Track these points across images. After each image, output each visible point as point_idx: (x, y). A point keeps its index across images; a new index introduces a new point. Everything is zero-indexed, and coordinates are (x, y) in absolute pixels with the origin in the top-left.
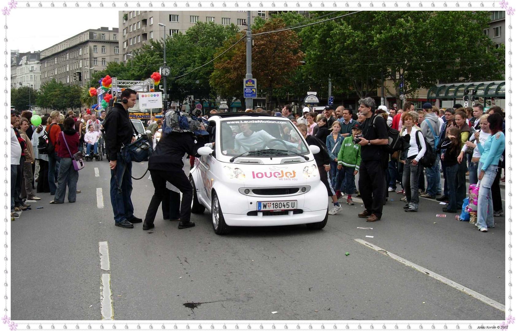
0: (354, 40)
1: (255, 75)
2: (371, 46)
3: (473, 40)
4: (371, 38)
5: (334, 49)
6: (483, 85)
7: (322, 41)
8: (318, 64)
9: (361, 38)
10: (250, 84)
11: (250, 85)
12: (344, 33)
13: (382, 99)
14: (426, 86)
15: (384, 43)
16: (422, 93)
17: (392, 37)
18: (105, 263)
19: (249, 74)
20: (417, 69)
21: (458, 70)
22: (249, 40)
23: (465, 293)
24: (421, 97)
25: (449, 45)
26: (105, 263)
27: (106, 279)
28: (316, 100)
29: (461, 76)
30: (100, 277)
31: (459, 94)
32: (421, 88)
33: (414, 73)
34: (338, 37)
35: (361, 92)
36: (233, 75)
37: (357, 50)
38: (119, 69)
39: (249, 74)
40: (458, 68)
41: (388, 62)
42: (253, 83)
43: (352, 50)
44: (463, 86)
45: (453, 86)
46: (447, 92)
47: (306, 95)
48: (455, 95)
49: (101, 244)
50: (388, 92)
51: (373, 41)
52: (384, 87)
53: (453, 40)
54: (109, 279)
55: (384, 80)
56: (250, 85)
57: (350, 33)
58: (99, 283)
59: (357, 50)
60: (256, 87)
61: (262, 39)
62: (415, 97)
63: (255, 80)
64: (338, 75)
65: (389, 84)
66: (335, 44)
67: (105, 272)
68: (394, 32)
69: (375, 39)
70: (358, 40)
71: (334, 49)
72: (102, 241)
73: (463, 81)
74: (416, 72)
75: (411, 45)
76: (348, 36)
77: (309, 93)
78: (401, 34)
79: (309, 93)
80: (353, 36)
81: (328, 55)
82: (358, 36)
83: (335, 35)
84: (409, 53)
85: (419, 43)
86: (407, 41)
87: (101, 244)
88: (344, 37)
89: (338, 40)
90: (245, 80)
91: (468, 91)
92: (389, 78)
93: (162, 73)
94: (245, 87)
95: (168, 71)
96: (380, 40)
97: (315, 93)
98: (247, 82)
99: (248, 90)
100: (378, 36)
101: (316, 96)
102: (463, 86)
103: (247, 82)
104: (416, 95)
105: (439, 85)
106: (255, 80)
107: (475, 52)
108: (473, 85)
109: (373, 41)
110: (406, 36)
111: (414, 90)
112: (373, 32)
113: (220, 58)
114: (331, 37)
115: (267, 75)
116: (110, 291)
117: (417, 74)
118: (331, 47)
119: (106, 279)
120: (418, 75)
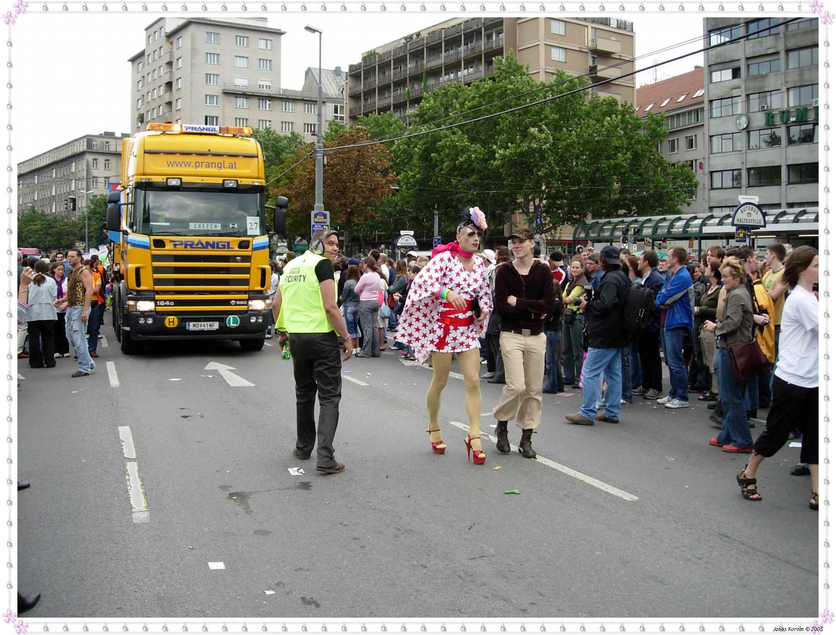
0: (470, 156)
3: (636, 157)
5: (442, 169)
6: (650, 220)
7: (425, 157)
8: (420, 190)
9: (480, 154)
10: (320, 219)
16: (566, 232)
17: (522, 154)
18: (129, 450)
19: (319, 205)
20: (558, 198)
21: (616, 200)
22: (319, 156)
23: (576, 478)
24: (564, 238)
25: (604, 164)
26: (129, 450)
27: (132, 468)
28: (413, 242)
29: (621, 209)
30: (125, 466)
34: (447, 151)
37: (474, 169)
39: (319, 205)
42: (325, 217)
43: (465, 171)
44: (623, 222)
45: (609, 223)
46: (602, 230)
47: (400, 235)
48: (612, 234)
49: (121, 429)
51: (495, 159)
53: (609, 158)
54: (136, 468)
55: (513, 213)
57: (465, 147)
58: (125, 472)
60: (328, 223)
62: (557, 238)
63: (328, 213)
64: (447, 206)
66: (443, 162)
67: (130, 460)
68: (524, 147)
71: (442, 169)
72: (122, 425)
73: (625, 215)
75: (549, 164)
76: (462, 150)
78: (534, 150)
79: (402, 232)
80: (469, 151)
81: (434, 178)
83: (443, 147)
84: (546, 176)
85: (562, 161)
86: (543, 158)
87: (121, 429)
88: (456, 152)
89: (448, 155)
90: (313, 213)
91: (627, 230)
92: (521, 211)
94: (313, 223)
96: (504, 157)
97: (412, 233)
98: (316, 217)
99: (317, 227)
100: (501, 152)
101: (414, 236)
103: (316, 217)
104: (558, 235)
105: (589, 220)
107: (640, 175)
108: (636, 221)
109: (495, 159)
112: (495, 147)
113: (278, 181)
114: (438, 152)
115: (345, 205)
116: (139, 480)
118: (437, 166)
119: (132, 468)
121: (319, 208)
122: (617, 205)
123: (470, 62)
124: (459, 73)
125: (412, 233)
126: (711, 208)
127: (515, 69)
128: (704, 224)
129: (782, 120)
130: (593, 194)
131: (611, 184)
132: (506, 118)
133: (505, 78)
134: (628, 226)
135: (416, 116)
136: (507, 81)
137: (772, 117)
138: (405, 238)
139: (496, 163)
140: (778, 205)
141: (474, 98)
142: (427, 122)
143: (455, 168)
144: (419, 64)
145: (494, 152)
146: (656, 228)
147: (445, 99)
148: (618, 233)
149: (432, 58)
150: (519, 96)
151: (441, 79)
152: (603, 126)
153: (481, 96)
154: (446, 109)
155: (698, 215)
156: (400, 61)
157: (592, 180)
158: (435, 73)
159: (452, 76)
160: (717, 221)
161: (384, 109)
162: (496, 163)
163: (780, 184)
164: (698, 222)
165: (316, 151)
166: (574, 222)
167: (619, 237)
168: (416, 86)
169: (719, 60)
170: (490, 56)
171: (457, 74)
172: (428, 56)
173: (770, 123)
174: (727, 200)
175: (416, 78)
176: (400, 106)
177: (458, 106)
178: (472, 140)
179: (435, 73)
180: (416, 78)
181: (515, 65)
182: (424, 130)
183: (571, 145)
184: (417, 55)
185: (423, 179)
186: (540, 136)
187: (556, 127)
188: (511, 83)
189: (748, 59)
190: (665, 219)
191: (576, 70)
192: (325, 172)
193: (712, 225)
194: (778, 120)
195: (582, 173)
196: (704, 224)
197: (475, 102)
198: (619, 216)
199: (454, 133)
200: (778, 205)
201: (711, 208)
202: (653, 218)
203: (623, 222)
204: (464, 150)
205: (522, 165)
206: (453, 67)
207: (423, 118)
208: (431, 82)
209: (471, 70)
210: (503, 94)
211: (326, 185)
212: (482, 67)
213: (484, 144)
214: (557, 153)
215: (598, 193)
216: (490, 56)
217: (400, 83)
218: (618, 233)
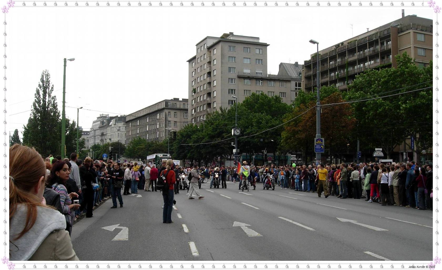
0: (385, 109)
1: (322, 135)
2: (398, 113)
4: (398, 107)
10: (319, 142)
11: (319, 142)
13: (404, 154)
19: (318, 135)
28: (382, 154)
35: (387, 149)
36: (303, 136)
38: (195, 129)
39: (318, 135)
42: (322, 141)
52: (405, 143)
56: (319, 142)
60: (323, 145)
61: (326, 109)
63: (323, 139)
70: (388, 108)
77: (376, 149)
79: (376, 149)
82: (388, 105)
83: (369, 104)
88: (377, 106)
89: (372, 109)
90: (315, 139)
92: (409, 137)
93: (234, 134)
94: (315, 144)
95: (238, 131)
96: (405, 109)
97: (381, 149)
99: (318, 147)
100: (404, 106)
101: (382, 151)
103: (317, 141)
109: (400, 110)
112: (400, 103)
113: (289, 123)
114: (366, 106)
121: (318, 136)
123: (372, 57)
124: (366, 64)
125: (381, 149)
138: (378, 152)
141: (385, 77)
144: (343, 59)
145: (400, 106)
149: (351, 56)
150: (411, 74)
151: (356, 67)
153: (389, 76)
156: (333, 58)
158: (353, 64)
159: (362, 65)
161: (326, 84)
165: (317, 106)
168: (342, 71)
170: (386, 53)
171: (364, 64)
172: (349, 54)
175: (342, 67)
176: (335, 82)
179: (353, 64)
180: (342, 67)
181: (408, 58)
182: (357, 94)
184: (342, 55)
188: (407, 68)
197: (386, 79)
199: (375, 97)
204: (381, 105)
206: (363, 60)
207: (357, 88)
208: (351, 69)
209: (372, 62)
210: (403, 74)
212: (378, 60)
213: (391, 101)
216: (386, 53)
217: (333, 70)
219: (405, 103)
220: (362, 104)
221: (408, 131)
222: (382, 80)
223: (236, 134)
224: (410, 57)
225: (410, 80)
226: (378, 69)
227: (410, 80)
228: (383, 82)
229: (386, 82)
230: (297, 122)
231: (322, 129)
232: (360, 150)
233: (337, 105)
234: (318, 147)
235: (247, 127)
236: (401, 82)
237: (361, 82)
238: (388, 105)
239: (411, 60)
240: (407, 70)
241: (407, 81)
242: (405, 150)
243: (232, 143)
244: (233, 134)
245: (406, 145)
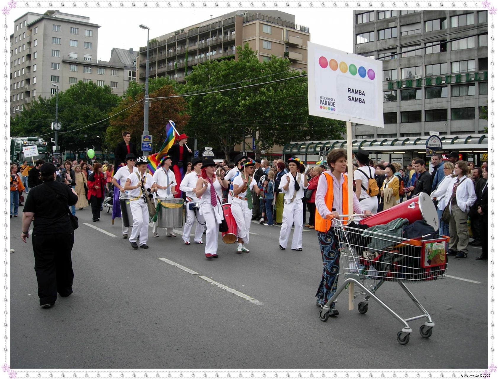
0: (224, 104)
5: (206, 112)
7: (196, 103)
8: (190, 123)
10: (147, 139)
12: (215, 98)
14: (277, 142)
15: (248, 108)
16: (277, 149)
17: (255, 103)
19: (146, 131)
22: (146, 102)
28: (212, 154)
31: (309, 150)
32: (274, 145)
33: (270, 133)
34: (210, 101)
37: (225, 112)
39: (146, 131)
40: (305, 129)
41: (251, 124)
42: (150, 139)
45: (304, 144)
46: (299, 149)
50: (250, 147)
52: (245, 143)
55: (245, 138)
59: (225, 112)
60: (152, 142)
62: (270, 152)
63: (151, 136)
65: (249, 141)
66: (206, 107)
69: (240, 104)
73: (310, 140)
74: (271, 131)
76: (219, 100)
77: (206, 148)
78: (263, 101)
79: (206, 148)
80: (223, 101)
81: (200, 116)
82: (227, 101)
83: (206, 98)
84: (269, 117)
85: (276, 108)
86: (268, 106)
88: (215, 101)
89: (210, 104)
90: (143, 136)
92: (249, 136)
94: (142, 142)
95: (59, 125)
96: (244, 105)
97: (211, 149)
99: (145, 145)
100: (243, 102)
102: (312, 143)
105: (292, 143)
106: (151, 136)
108: (321, 143)
109: (239, 106)
110: (268, 103)
111: (269, 147)
112: (239, 99)
114: (203, 101)
115: (159, 132)
117: (272, 133)
118: (202, 109)
120: (274, 135)
122: (306, 134)
123: (215, 47)
124: (207, 54)
125: (211, 149)
126: (356, 136)
127: (247, 53)
128: (361, 145)
129: (398, 86)
130: (293, 127)
131: (305, 122)
132: (246, 83)
133: (244, 59)
134: (325, 146)
135: (191, 79)
136: (245, 61)
137: (393, 84)
138: (208, 152)
139: (240, 108)
140: (395, 135)
141: (225, 70)
142: (197, 83)
143: (214, 111)
144: (183, 48)
146: (333, 147)
147: (207, 69)
148: (318, 149)
149: (192, 45)
150: (253, 69)
151: (196, 57)
152: (301, 88)
153: (229, 69)
154: (207, 76)
155: (358, 140)
156: (172, 46)
157: (294, 120)
158: (193, 53)
159: (203, 56)
160: (369, 143)
162: (240, 108)
163: (396, 122)
164: (359, 144)
165: (145, 99)
166: (281, 144)
167: (303, 152)
168: (181, 61)
169: (362, 51)
170: (230, 44)
171: (206, 55)
173: (391, 88)
174: (365, 131)
175: (181, 56)
177: (215, 73)
178: (224, 94)
179: (193, 53)
180: (181, 56)
181: (250, 51)
183: (283, 99)
184: (182, 43)
185: (193, 117)
186: (267, 93)
187: (275, 89)
188: (248, 62)
189: (378, 51)
190: (338, 142)
191: (279, 53)
192: (150, 111)
193: (377, 145)
194: (395, 87)
195: (288, 115)
196: (361, 145)
198: (307, 140)
199: (213, 90)
200: (395, 135)
201: (356, 136)
202: (331, 141)
203: (312, 143)
205: (254, 109)
206: (204, 50)
207: (194, 80)
208: (190, 59)
209: (214, 53)
210: (243, 68)
211: (150, 120)
212: (221, 51)
214: (274, 103)
215: (296, 126)
216: (230, 44)
218: (309, 150)
219: (245, 99)
220: (199, 99)
221: (248, 129)
222: (223, 73)
223: (56, 128)
224: (252, 50)
225: (252, 75)
226: (219, 61)
227: (252, 75)
228: (223, 76)
229: (226, 76)
230: (124, 116)
231: (149, 125)
232: (197, 150)
233: (168, 99)
234: (145, 145)
235: (71, 121)
236: (242, 77)
237: (199, 75)
238: (227, 101)
239: (253, 52)
240: (248, 64)
241: (248, 76)
242: (244, 149)
243: (52, 139)
244: (52, 128)
245: (246, 145)
